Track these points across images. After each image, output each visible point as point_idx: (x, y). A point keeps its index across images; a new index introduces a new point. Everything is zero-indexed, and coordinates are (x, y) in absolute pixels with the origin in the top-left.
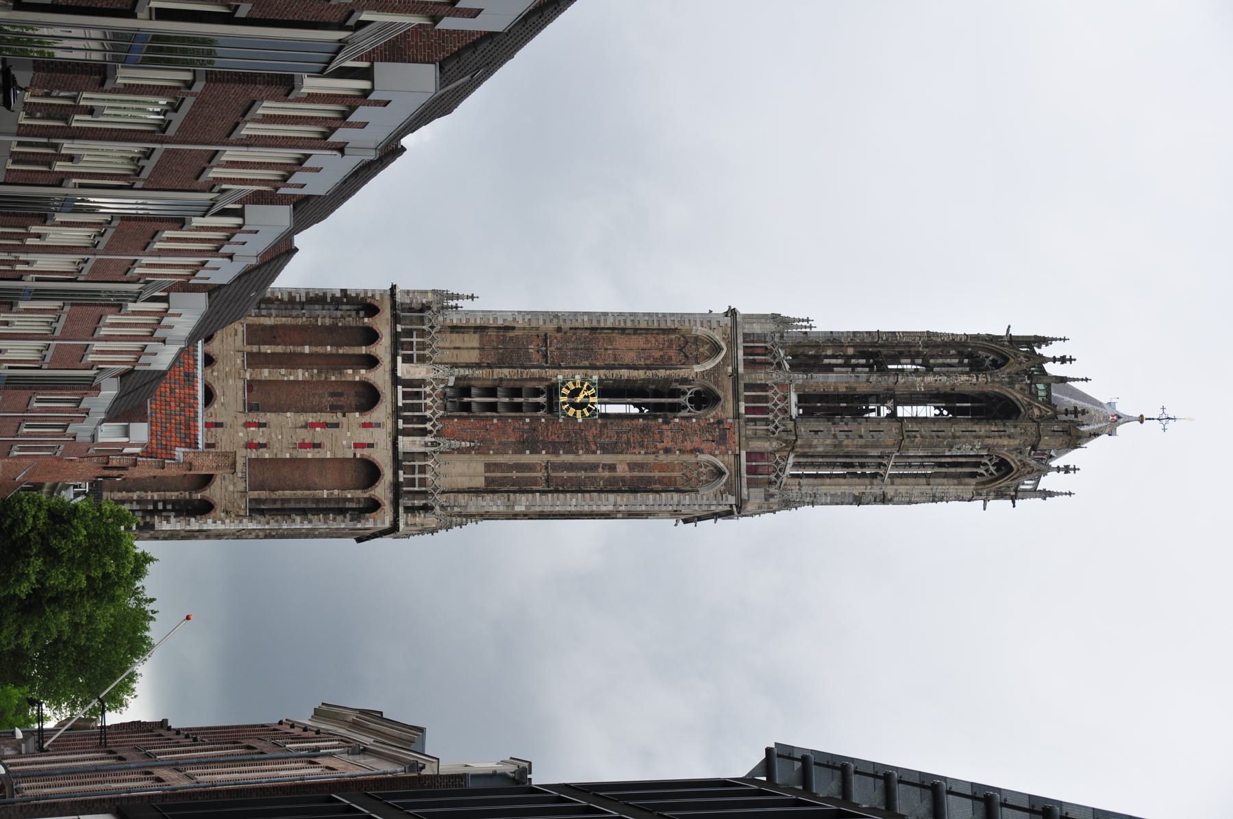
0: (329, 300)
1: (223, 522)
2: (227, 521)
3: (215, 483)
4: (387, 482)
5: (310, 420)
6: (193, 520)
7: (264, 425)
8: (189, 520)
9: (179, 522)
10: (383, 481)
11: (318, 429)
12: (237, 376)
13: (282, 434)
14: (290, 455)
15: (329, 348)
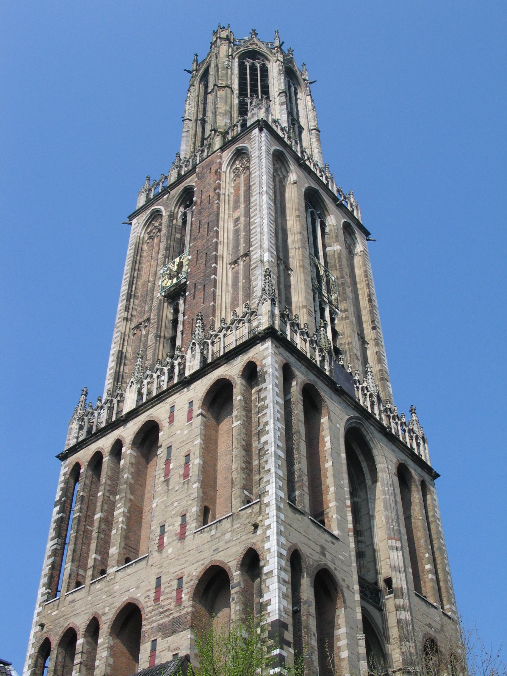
0: (61, 515)
1: (269, 527)
2: (267, 522)
3: (221, 559)
4: (226, 369)
5: (162, 479)
6: (265, 570)
7: (163, 527)
8: (266, 574)
9: (268, 587)
10: (224, 374)
11: (171, 466)
12: (112, 582)
13: (173, 503)
14: (195, 483)
15: (100, 494)
